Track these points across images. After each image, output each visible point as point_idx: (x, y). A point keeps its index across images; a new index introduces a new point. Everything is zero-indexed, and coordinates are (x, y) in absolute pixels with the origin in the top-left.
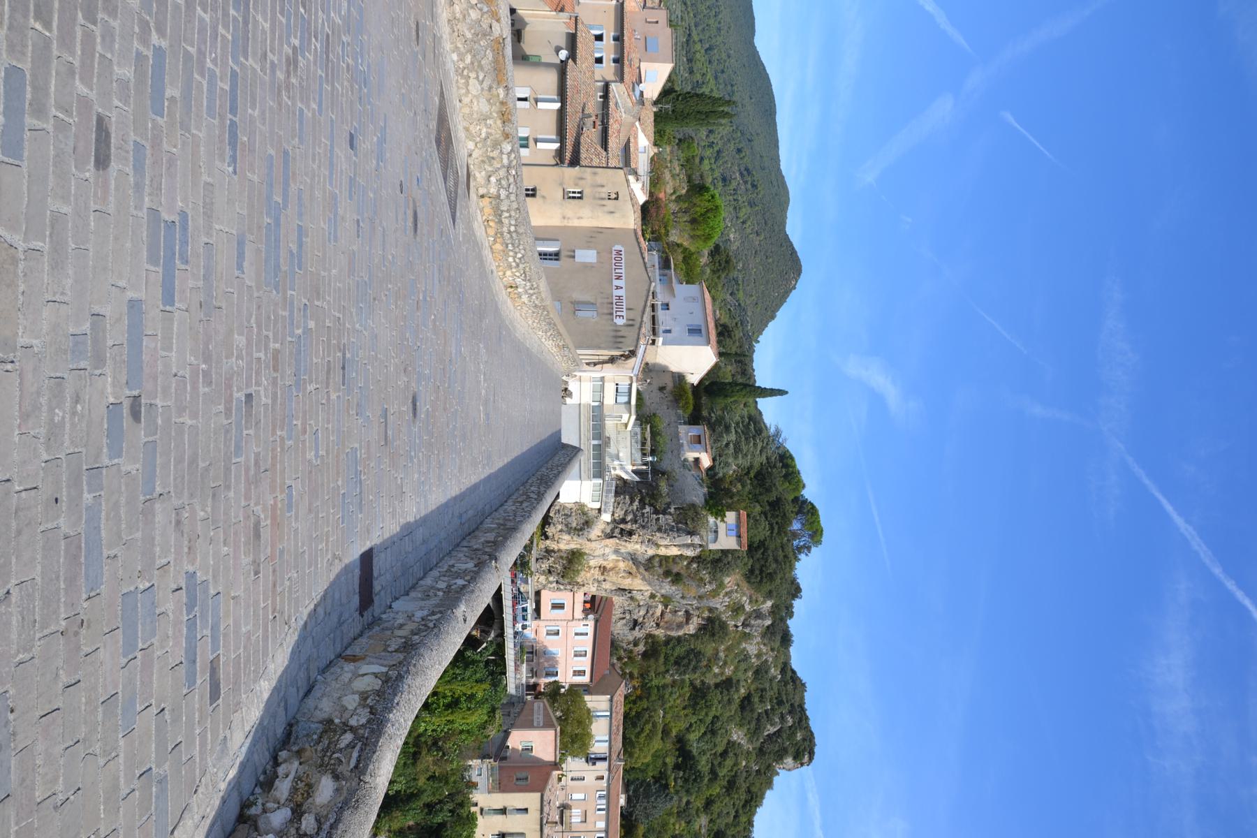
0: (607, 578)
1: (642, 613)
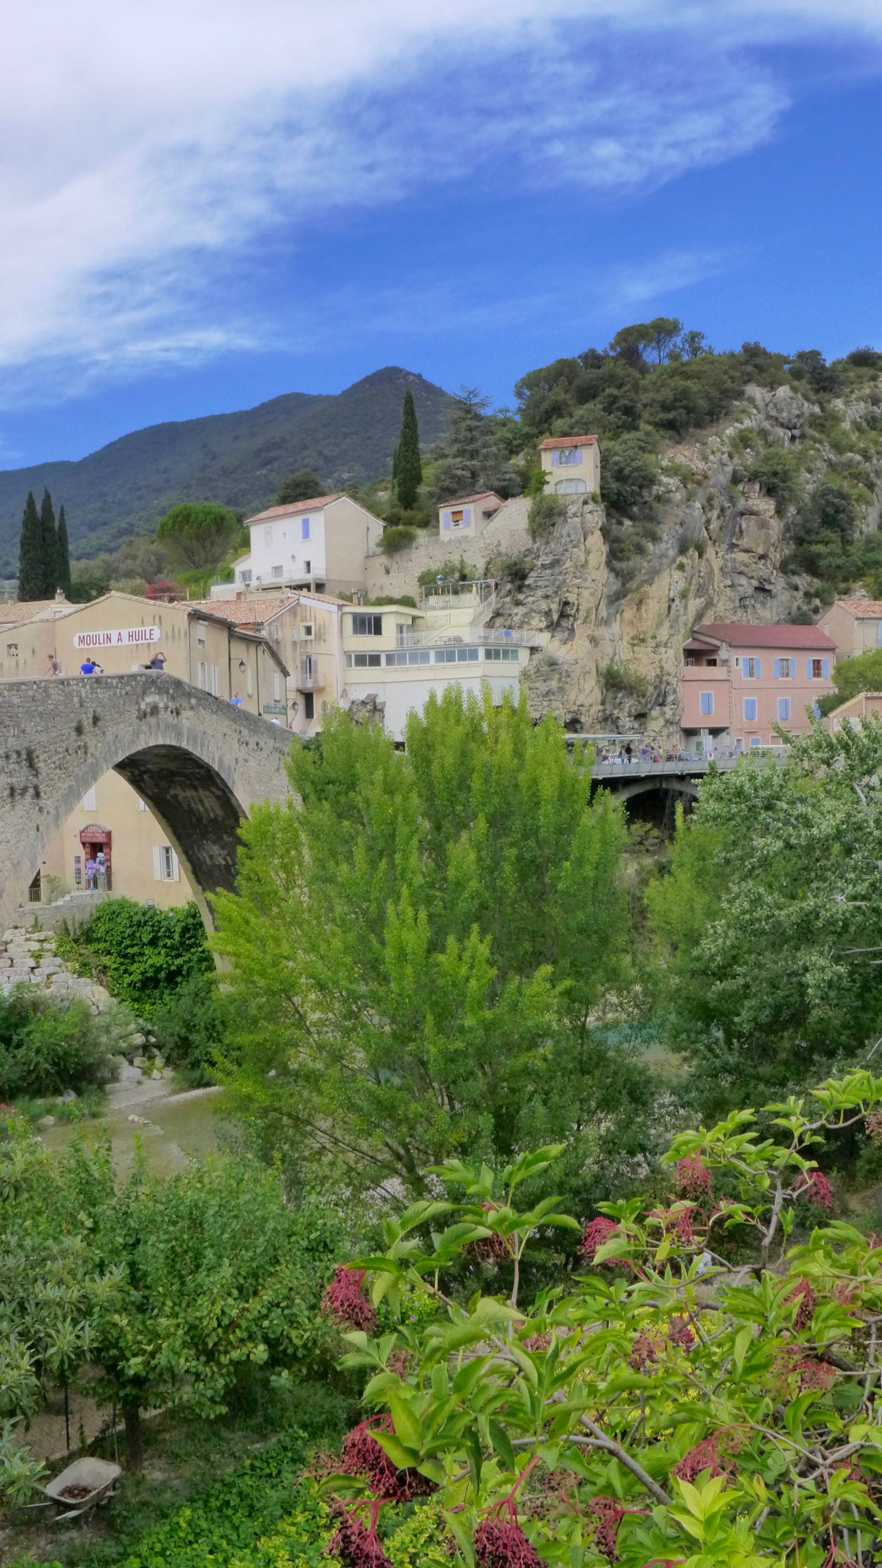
0: (650, 634)
1: (743, 581)
